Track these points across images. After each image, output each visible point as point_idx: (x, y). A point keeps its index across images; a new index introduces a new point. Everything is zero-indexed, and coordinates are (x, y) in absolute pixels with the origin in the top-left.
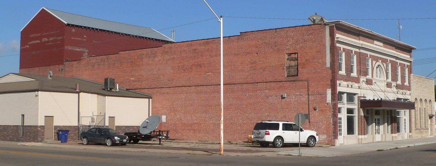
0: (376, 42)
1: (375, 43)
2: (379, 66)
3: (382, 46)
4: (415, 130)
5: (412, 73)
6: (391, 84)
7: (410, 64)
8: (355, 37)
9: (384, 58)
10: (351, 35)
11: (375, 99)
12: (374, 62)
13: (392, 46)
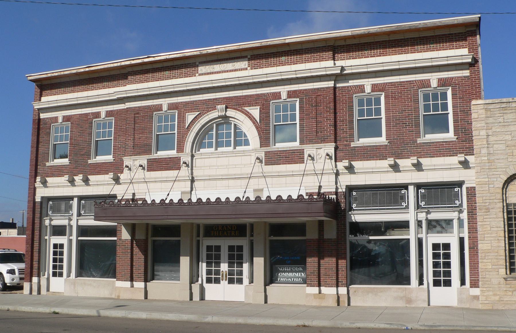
0: (202, 69)
1: (200, 72)
2: (230, 119)
3: (247, 66)
4: (505, 279)
5: (479, 97)
7: (468, 71)
10: (76, 88)
12: (190, 117)
13: (317, 52)
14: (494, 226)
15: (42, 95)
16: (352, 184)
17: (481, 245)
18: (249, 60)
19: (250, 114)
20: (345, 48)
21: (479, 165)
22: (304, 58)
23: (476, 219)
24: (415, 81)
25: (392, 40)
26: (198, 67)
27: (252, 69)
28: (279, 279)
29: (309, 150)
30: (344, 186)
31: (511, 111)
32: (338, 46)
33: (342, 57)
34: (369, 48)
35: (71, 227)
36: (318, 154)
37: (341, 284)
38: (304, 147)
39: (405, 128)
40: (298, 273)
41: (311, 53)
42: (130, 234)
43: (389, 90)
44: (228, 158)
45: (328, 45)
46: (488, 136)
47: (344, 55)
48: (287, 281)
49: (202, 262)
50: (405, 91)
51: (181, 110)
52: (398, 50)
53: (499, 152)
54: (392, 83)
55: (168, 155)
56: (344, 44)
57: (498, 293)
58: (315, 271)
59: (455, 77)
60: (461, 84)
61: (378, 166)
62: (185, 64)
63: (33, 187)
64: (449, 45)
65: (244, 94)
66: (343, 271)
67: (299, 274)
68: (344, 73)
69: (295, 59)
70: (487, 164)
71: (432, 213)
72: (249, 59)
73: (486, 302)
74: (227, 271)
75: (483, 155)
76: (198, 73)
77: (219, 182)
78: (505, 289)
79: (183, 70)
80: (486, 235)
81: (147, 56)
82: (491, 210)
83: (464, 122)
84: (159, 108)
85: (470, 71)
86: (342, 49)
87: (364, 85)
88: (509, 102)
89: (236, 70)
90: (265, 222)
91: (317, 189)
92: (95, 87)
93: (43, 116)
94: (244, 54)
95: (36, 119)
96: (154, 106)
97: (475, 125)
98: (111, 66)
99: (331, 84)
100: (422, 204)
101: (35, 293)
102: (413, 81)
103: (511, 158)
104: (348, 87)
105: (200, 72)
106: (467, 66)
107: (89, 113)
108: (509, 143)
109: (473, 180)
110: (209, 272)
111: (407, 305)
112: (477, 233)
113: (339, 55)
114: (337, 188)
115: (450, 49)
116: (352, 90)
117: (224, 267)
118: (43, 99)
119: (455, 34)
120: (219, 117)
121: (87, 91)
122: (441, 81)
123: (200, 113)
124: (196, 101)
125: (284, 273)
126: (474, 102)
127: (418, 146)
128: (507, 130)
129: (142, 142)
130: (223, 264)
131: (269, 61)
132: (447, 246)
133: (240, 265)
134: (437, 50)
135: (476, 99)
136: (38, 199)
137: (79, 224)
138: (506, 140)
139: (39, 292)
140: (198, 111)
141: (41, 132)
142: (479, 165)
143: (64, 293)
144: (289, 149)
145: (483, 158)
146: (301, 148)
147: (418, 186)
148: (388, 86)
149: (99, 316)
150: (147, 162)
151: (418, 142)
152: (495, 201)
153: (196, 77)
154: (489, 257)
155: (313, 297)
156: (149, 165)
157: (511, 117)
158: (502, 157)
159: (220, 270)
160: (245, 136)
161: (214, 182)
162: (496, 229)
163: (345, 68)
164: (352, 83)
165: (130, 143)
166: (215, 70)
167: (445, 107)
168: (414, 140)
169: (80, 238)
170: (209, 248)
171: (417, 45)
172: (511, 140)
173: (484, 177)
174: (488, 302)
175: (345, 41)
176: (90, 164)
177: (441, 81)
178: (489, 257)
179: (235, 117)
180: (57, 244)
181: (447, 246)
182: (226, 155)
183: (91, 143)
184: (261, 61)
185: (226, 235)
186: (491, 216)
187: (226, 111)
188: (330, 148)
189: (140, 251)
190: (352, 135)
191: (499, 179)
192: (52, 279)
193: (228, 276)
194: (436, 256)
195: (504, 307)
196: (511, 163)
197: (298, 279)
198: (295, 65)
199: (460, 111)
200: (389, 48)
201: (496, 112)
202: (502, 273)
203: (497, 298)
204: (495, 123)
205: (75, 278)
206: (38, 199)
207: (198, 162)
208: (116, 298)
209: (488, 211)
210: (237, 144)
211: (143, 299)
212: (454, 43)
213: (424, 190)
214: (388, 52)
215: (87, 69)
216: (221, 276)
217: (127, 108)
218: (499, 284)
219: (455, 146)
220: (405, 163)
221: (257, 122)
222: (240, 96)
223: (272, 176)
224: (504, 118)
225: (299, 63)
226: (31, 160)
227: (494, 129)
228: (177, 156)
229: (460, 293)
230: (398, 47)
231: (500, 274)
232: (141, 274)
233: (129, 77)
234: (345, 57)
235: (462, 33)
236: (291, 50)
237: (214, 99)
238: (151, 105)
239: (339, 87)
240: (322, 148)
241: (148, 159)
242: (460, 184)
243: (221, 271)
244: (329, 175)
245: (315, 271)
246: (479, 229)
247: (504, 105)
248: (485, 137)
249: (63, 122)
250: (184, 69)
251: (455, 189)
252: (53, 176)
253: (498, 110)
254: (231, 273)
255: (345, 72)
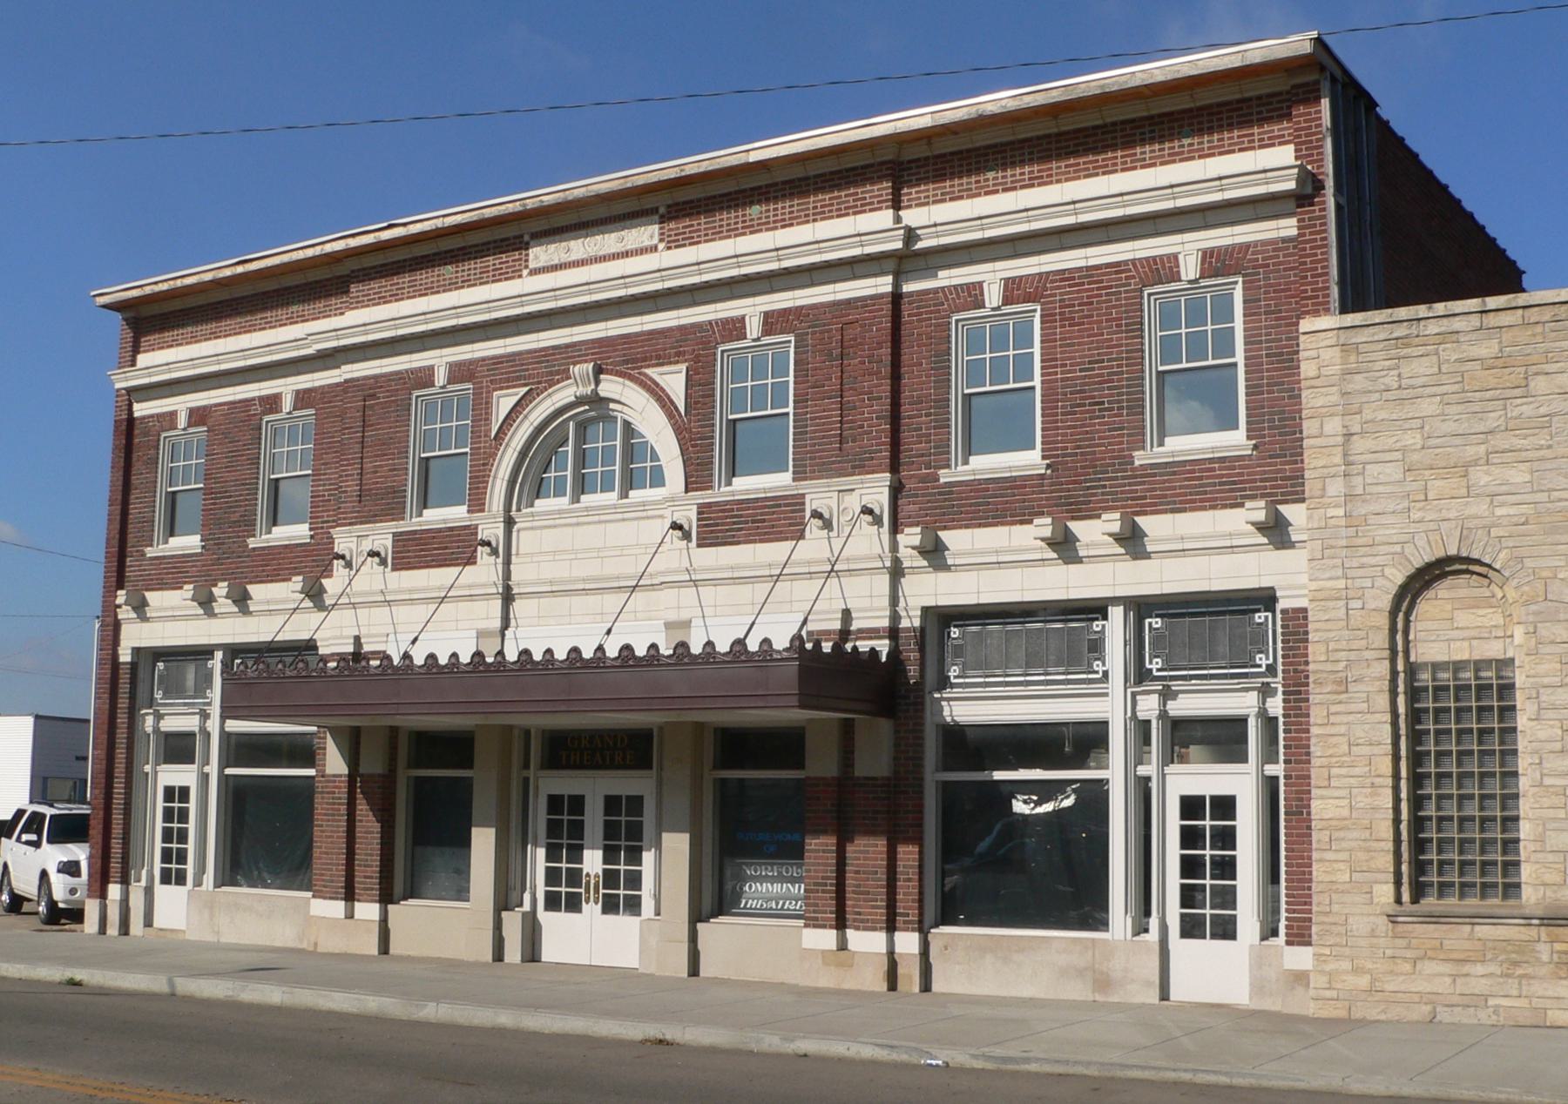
0: (540, 254)
1: (532, 265)
2: (612, 406)
3: (655, 240)
4: (1392, 918)
6: (798, 502)
7: (1293, 221)
8: (320, 305)
9: (670, 329)
11: (460, 657)
12: (504, 402)
13: (848, 185)
14: (1360, 741)
15: (140, 347)
16: (940, 604)
17: (1319, 802)
18: (663, 220)
19: (663, 390)
20: (931, 168)
21: (1317, 534)
22: (811, 206)
23: (1308, 715)
24: (1133, 261)
25: (1067, 133)
26: (527, 249)
27: (669, 248)
28: (744, 901)
29: (820, 495)
30: (837, 612)
31: (1421, 351)
32: (910, 162)
33: (922, 195)
34: (1000, 162)
35: (208, 735)
36: (845, 509)
37: (905, 922)
38: (805, 487)
39: (1098, 417)
40: (797, 885)
41: (832, 188)
42: (347, 758)
43: (1055, 295)
44: (603, 525)
45: (879, 160)
46: (1348, 435)
47: (928, 190)
48: (766, 909)
49: (536, 845)
50: (1101, 295)
51: (482, 382)
52: (1084, 163)
53: (1381, 489)
54: (1063, 271)
55: (445, 521)
56: (930, 154)
57: (1369, 965)
58: (828, 878)
59: (1256, 244)
60: (1274, 264)
61: (1015, 543)
62: (495, 242)
63: (110, 620)
64: (1239, 137)
65: (647, 328)
66: (909, 880)
67: (800, 887)
68: (916, 247)
69: (787, 210)
70: (1343, 532)
71: (1180, 696)
72: (662, 216)
73: (1328, 994)
74: (601, 874)
75: (1330, 500)
76: (526, 267)
77: (577, 601)
78: (1389, 952)
79: (489, 261)
80: (1334, 771)
81: (385, 224)
82: (1352, 687)
83: (1279, 391)
84: (424, 378)
85: (1299, 221)
86: (922, 170)
87: (980, 284)
88: (1419, 320)
89: (626, 254)
90: (699, 727)
91: (885, 617)
92: (269, 319)
93: (141, 409)
94: (649, 202)
95: (121, 421)
96: (412, 374)
97: (1311, 399)
98: (299, 258)
99: (882, 284)
100: (1155, 665)
101: (113, 930)
102: (1126, 262)
103: (1420, 509)
104: (935, 291)
105: (532, 265)
106: (1291, 205)
107: (253, 399)
108: (1416, 457)
109: (1303, 587)
110: (552, 876)
111: (1098, 998)
112: (1309, 762)
113: (913, 190)
114: (895, 617)
115: (1241, 150)
116: (947, 300)
117: (593, 862)
118: (143, 360)
119: (1259, 98)
120: (579, 401)
121: (249, 331)
122: (1211, 257)
123: (531, 389)
124: (520, 353)
125: (758, 884)
126: (1306, 325)
127: (1135, 477)
128: (1410, 415)
129: (382, 483)
130: (591, 851)
131: (715, 221)
132: (1225, 806)
133: (635, 856)
134: (1200, 157)
135: (1316, 313)
136: (125, 657)
137: (227, 729)
138: (1404, 450)
139: (125, 928)
140: (525, 385)
141: (135, 456)
142: (1317, 534)
143: (184, 932)
144: (763, 495)
145: (1331, 512)
146: (796, 492)
147: (1140, 607)
148: (1052, 281)
149: (173, 995)
150: (394, 541)
151: (1137, 463)
152: (1368, 655)
153: (520, 280)
154: (1344, 845)
155: (820, 961)
156: (398, 552)
157: (1422, 370)
158: (1391, 508)
159: (581, 870)
160: (655, 457)
161: (565, 601)
162: (1365, 750)
163: (919, 232)
164: (948, 278)
165: (352, 486)
166: (574, 257)
167: (1224, 343)
168: (1125, 457)
169: (229, 771)
170: (555, 803)
171: (1143, 142)
172: (1423, 448)
173: (1333, 573)
174: (1334, 994)
175: (929, 144)
176: (254, 549)
177: (1211, 257)
178: (1344, 845)
179: (623, 400)
180: (174, 788)
181: (1225, 806)
182: (596, 518)
183: (257, 489)
184: (695, 223)
185: (600, 762)
186: (1353, 707)
187: (597, 382)
188: (875, 490)
189: (371, 810)
190: (944, 447)
191: (1380, 582)
192: (161, 891)
193: (604, 888)
194: (1190, 837)
195: (1384, 1011)
196: (1422, 527)
197: (796, 905)
198: (787, 229)
199: (1268, 356)
200: (1059, 157)
201: (1373, 356)
202: (1383, 900)
203: (1363, 982)
204: (1370, 392)
205: (215, 887)
206: (125, 657)
207: (524, 541)
208: (311, 949)
209: (1343, 688)
210: (630, 482)
211: (376, 952)
212: (1256, 130)
213: (1159, 620)
214: (1054, 171)
215: (240, 269)
216: (582, 890)
217: (346, 381)
218: (1373, 934)
219: (1248, 474)
220: (1094, 532)
221: (680, 414)
222: (637, 334)
223: (715, 582)
224: (1399, 375)
225: (798, 224)
226: (108, 539)
227: (1368, 414)
228: (468, 523)
229: (1258, 962)
230: (1086, 152)
231: (1376, 900)
232: (371, 877)
233: (353, 288)
234: (928, 197)
235: (1280, 94)
236: (776, 184)
237: (567, 346)
238: (407, 371)
239: (911, 294)
240: (853, 490)
241: (394, 534)
242: (1267, 599)
243: (584, 873)
244: (871, 574)
245: (828, 878)
246: (1316, 749)
247: (1400, 331)
248: (1340, 440)
249: (189, 426)
250: (491, 258)
251: (1257, 615)
252: (161, 586)
253: (1381, 345)
254: (610, 878)
255: (920, 245)
